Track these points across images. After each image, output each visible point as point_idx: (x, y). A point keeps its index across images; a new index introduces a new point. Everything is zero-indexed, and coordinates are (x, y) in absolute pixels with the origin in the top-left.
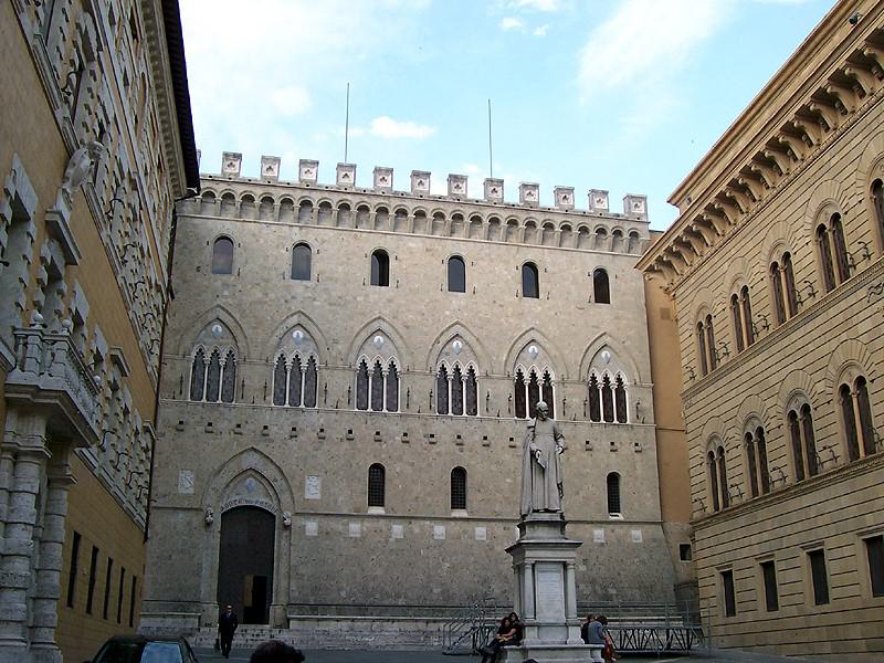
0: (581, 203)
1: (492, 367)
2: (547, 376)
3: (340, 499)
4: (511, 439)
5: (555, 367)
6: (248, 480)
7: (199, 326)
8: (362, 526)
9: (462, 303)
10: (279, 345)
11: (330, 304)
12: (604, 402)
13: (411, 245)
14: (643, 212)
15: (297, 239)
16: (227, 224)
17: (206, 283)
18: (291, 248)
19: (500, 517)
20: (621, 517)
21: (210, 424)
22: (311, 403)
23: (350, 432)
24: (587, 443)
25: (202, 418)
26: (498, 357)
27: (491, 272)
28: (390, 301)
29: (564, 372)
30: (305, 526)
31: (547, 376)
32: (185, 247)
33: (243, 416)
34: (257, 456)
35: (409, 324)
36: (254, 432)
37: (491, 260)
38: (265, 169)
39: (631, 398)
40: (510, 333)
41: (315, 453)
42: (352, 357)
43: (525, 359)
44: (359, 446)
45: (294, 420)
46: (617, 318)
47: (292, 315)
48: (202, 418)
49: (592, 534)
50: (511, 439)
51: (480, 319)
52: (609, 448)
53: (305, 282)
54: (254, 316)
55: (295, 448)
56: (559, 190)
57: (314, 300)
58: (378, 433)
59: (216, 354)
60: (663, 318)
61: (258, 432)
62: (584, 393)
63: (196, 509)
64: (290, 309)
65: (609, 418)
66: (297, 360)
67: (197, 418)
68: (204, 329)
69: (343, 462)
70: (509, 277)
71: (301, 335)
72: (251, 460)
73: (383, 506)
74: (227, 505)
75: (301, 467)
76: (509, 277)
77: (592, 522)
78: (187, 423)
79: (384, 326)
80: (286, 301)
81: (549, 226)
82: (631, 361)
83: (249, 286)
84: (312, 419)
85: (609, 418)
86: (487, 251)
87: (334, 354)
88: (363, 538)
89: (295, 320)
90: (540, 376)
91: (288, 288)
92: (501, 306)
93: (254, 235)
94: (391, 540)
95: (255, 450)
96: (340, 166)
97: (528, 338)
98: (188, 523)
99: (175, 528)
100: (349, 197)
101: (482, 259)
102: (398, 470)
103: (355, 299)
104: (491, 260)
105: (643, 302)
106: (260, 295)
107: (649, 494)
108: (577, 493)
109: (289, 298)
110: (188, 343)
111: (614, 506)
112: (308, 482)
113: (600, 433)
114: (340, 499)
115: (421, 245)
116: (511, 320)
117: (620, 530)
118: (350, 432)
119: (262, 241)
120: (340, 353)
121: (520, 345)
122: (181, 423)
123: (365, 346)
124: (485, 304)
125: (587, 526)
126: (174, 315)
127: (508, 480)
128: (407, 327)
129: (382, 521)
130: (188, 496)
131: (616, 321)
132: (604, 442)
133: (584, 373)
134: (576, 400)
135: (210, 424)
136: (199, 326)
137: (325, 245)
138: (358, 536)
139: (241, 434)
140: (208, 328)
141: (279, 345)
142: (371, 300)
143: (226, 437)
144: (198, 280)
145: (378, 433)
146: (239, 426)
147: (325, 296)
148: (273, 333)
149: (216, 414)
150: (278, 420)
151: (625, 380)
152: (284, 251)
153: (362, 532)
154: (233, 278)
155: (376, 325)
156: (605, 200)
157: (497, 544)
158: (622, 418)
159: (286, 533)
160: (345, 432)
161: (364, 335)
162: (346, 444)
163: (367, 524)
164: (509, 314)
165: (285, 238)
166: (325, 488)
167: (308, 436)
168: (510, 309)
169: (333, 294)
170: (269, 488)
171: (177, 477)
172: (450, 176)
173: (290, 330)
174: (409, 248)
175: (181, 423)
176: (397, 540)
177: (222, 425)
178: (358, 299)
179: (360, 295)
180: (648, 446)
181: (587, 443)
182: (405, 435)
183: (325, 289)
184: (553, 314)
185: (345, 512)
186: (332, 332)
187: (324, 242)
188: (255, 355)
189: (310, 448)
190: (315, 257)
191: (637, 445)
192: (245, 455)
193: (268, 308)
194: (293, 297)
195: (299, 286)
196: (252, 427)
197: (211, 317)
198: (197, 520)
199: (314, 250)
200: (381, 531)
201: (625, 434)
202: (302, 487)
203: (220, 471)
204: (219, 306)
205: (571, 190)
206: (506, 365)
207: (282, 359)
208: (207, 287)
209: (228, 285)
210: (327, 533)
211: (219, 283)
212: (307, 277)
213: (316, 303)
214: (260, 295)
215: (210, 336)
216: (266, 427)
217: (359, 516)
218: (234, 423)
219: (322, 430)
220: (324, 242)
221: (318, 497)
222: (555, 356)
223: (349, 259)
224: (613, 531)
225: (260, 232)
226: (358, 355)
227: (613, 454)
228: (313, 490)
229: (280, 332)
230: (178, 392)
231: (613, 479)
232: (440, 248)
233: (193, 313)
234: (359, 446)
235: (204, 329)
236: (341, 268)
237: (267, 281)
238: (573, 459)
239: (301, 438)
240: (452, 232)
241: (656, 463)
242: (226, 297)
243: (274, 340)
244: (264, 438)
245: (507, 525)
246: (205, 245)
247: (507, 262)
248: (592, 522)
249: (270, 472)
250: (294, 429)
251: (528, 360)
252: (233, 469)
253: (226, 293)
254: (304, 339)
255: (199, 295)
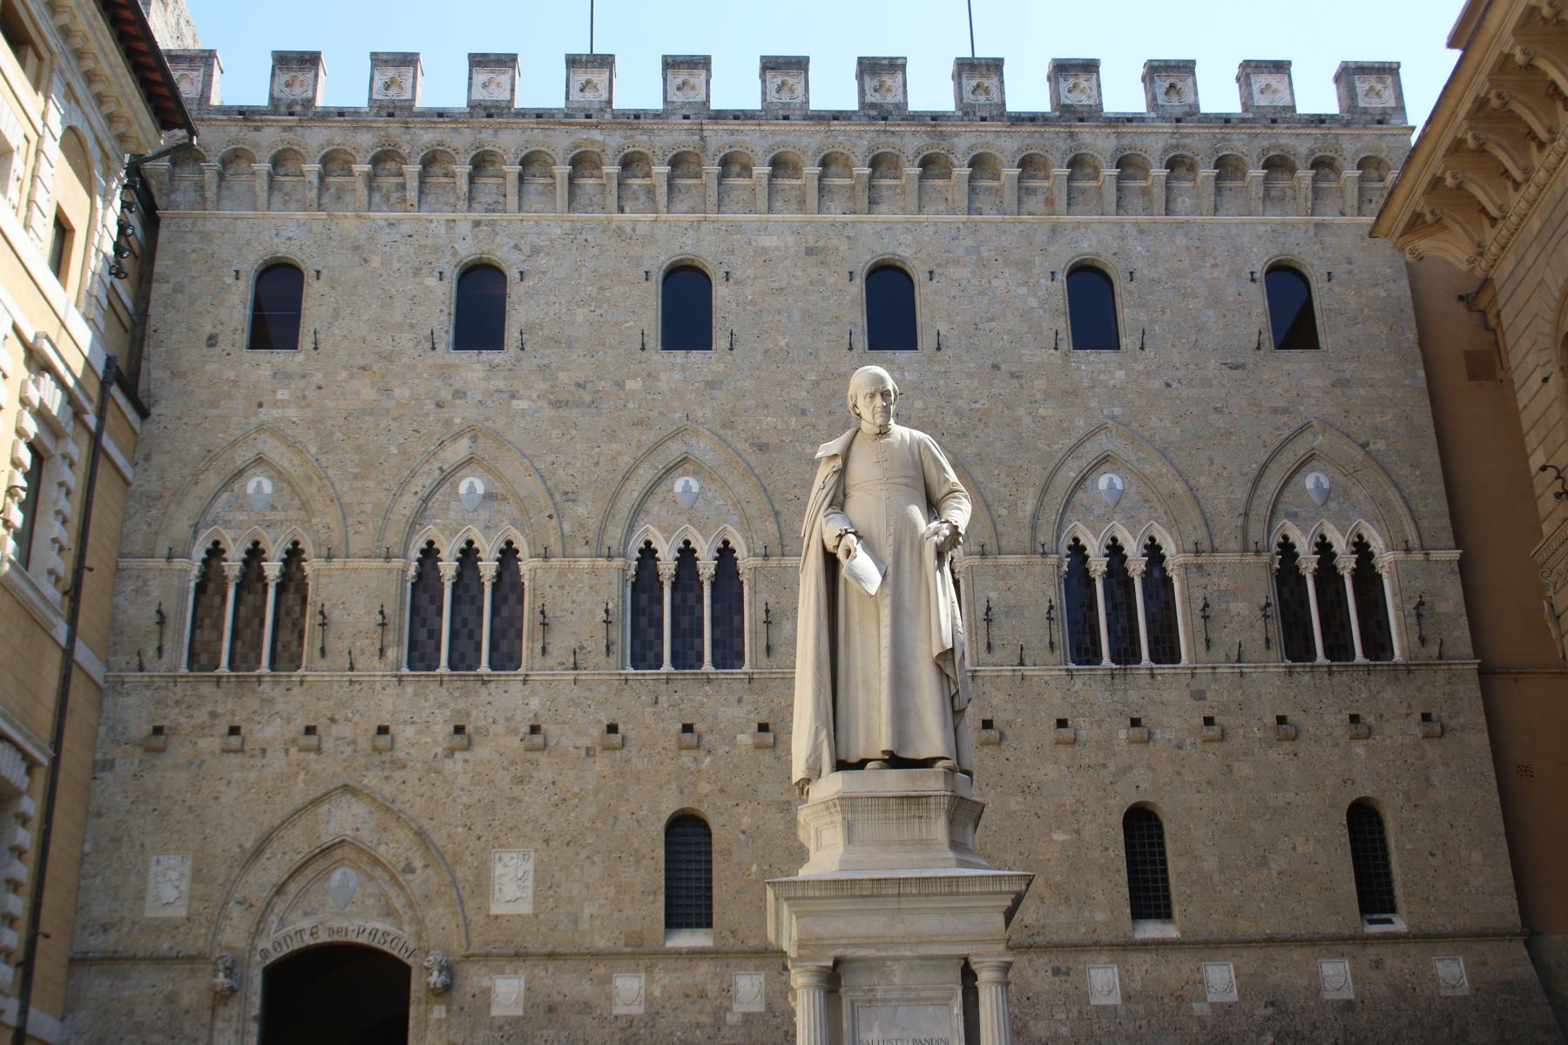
0: (1218, 95)
1: (998, 535)
2: (1153, 552)
3: (588, 910)
4: (1062, 723)
5: (1174, 524)
6: (336, 877)
7: (212, 481)
8: (650, 980)
9: (908, 376)
10: (418, 519)
11: (556, 404)
12: (1320, 611)
13: (766, 241)
14: (1392, 103)
15: (468, 250)
16: (286, 229)
17: (232, 375)
18: (452, 274)
19: (1038, 939)
20: (1399, 925)
21: (234, 731)
22: (506, 658)
23: (612, 729)
24: (1281, 720)
25: (213, 715)
26: (1012, 508)
27: (983, 293)
28: (711, 385)
29: (1201, 534)
30: (489, 989)
31: (1153, 552)
32: (179, 289)
33: (322, 704)
34: (359, 808)
35: (764, 440)
36: (354, 742)
37: (983, 264)
38: (378, 84)
39: (1399, 591)
40: (1041, 444)
41: (517, 791)
42: (615, 535)
43: (1089, 510)
44: (638, 763)
45: (461, 704)
46: (1341, 383)
47: (456, 437)
48: (213, 715)
49: (1316, 975)
50: (1062, 723)
51: (958, 413)
52: (1341, 730)
53: (487, 355)
54: (358, 449)
55: (463, 780)
56: (1155, 70)
57: (513, 397)
58: (688, 728)
59: (255, 554)
60: (1473, 375)
61: (364, 744)
62: (1264, 589)
63: (191, 959)
64: (448, 423)
65: (1338, 648)
66: (469, 555)
67: (202, 716)
68: (226, 486)
69: (592, 810)
70: (1033, 302)
71: (480, 489)
72: (345, 818)
73: (709, 925)
74: (277, 945)
75: (478, 829)
76: (1033, 302)
77: (1312, 941)
78: (174, 731)
79: (702, 447)
80: (438, 405)
81: (1127, 164)
82: (1392, 494)
83: (344, 374)
84: (503, 701)
85: (1338, 648)
86: (969, 242)
87: (567, 527)
88: (653, 1014)
89: (462, 448)
90: (1133, 549)
91: (443, 372)
92: (1013, 375)
93: (356, 248)
94: (731, 1018)
95: (346, 788)
96: (573, 62)
97: (1091, 451)
98: (171, 999)
99: (131, 1012)
100: (596, 135)
101: (957, 262)
102: (746, 821)
103: (620, 385)
104: (983, 264)
105: (1412, 335)
106: (369, 394)
107: (1476, 857)
108: (1263, 862)
109: (446, 395)
110: (182, 527)
111: (1375, 893)
112: (499, 869)
113: (1319, 695)
114: (588, 910)
115: (791, 240)
116: (1042, 412)
117: (1396, 963)
118: (612, 729)
119: (376, 261)
120: (582, 526)
121: (1070, 473)
122: (158, 731)
123: (654, 507)
124: (970, 375)
125: (1297, 954)
126: (147, 458)
127: (1058, 837)
128: (762, 448)
129: (704, 968)
130: (172, 926)
131: (1338, 391)
132: (1329, 718)
133: (1256, 532)
134: (1239, 607)
135: (234, 731)
136: (212, 481)
137: (542, 261)
138: (638, 1010)
139: (319, 750)
140: (237, 486)
141: (418, 519)
142: (663, 385)
143: (277, 762)
144: (210, 367)
145: (688, 728)
146: (310, 730)
147: (543, 386)
148: (403, 485)
149: (252, 702)
150: (421, 708)
151: (1377, 543)
152: (432, 281)
153: (649, 1000)
154: (300, 357)
155: (675, 449)
156: (1283, 87)
157: (1037, 1018)
158: (1378, 644)
159: (439, 1012)
160: (596, 732)
161: (645, 475)
162: (602, 763)
163: (667, 980)
164: (1039, 396)
165: (436, 249)
166: (545, 883)
167: (498, 746)
168: (1040, 384)
169: (561, 375)
170: (393, 893)
171: (144, 878)
172: (861, 60)
173: (448, 477)
174: (764, 250)
175: (158, 731)
176: (748, 1018)
177: (269, 731)
178: (630, 385)
179: (634, 377)
180: (1462, 720)
181: (1281, 720)
182: (763, 728)
183: (542, 368)
184: (1157, 384)
185: (601, 944)
186: (561, 474)
187: (536, 251)
188: (357, 543)
189: (503, 779)
190: (516, 292)
191: (1426, 717)
192: (324, 808)
193: (393, 424)
194: (459, 394)
195: (474, 365)
196: (345, 730)
197: (243, 456)
198: (191, 989)
199: (512, 274)
200: (703, 995)
201: (1389, 693)
202: (482, 883)
203: (258, 852)
204: (260, 428)
205: (1187, 67)
206: (1034, 528)
207: (430, 553)
208: (235, 383)
209: (288, 376)
210: (551, 1009)
211: (265, 372)
212: (496, 343)
213: (519, 404)
214: (369, 394)
215: (241, 508)
216: (383, 730)
217: (638, 954)
218: (299, 724)
219: (535, 729)
220: (536, 251)
221: (526, 908)
222: (1173, 495)
223: (602, 289)
224: (1378, 964)
225: (371, 239)
226: (631, 529)
227: (1360, 749)
228: (512, 886)
229: (423, 482)
230: (151, 652)
231: (1364, 823)
232: (844, 246)
233: (195, 449)
234: (638, 763)
235: (226, 486)
236: (580, 314)
237: (389, 358)
238: (1244, 769)
239: (482, 752)
240: (873, 202)
241: (1488, 764)
242: (282, 405)
243: (408, 504)
244: (377, 759)
245: (1062, 960)
246: (230, 280)
247: (1025, 265)
248: (1312, 941)
249: (395, 847)
250: (459, 730)
251: (1098, 511)
252: (297, 843)
253: (282, 394)
254: (489, 496)
255: (214, 404)
